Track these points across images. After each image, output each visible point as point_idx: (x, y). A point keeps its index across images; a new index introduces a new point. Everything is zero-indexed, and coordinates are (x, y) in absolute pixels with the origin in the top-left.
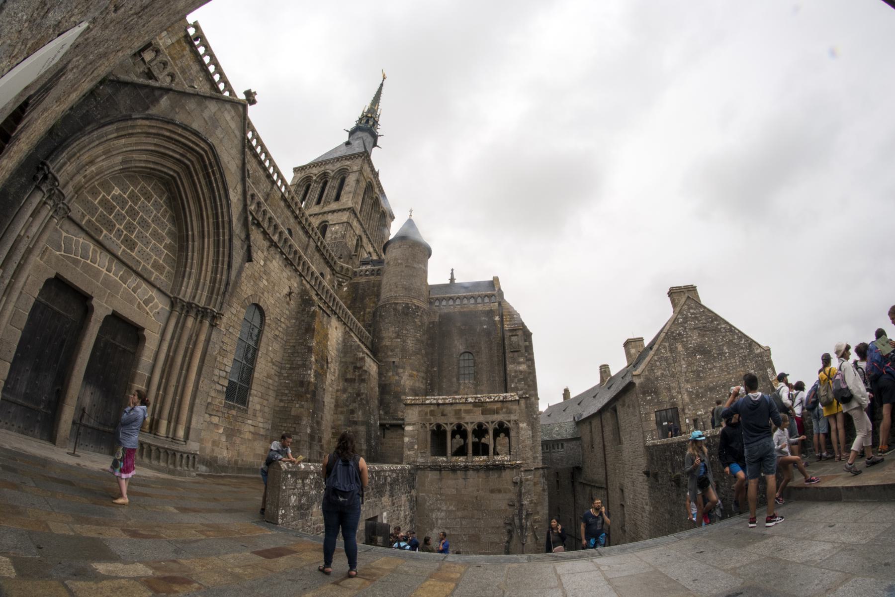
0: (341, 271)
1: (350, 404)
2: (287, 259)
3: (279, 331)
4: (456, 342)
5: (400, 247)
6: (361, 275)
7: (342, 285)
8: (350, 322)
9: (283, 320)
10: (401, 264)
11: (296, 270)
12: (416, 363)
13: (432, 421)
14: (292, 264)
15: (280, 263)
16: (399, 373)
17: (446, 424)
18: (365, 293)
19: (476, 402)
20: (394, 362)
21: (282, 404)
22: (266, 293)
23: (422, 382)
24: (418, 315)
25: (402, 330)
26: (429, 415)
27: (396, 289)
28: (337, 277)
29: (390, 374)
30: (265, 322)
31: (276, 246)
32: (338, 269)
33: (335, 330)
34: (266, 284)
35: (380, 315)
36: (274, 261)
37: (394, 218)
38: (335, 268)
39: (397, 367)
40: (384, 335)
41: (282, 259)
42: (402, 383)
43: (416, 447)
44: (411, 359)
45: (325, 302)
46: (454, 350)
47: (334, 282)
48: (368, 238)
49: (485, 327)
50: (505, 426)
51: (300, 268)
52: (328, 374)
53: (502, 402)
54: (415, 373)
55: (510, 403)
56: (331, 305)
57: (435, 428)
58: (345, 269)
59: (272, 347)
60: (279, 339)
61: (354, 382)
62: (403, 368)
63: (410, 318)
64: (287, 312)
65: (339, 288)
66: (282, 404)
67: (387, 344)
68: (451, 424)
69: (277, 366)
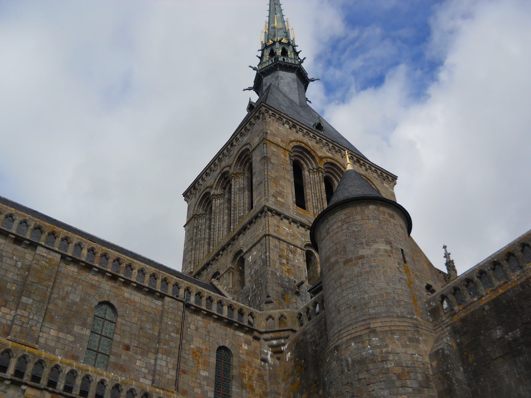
7: (281, 352)
10: (337, 262)
24: (388, 353)
28: (266, 340)
32: (261, 325)
38: (255, 327)
47: (262, 352)
58: (276, 318)
63: (371, 366)
65: (278, 359)
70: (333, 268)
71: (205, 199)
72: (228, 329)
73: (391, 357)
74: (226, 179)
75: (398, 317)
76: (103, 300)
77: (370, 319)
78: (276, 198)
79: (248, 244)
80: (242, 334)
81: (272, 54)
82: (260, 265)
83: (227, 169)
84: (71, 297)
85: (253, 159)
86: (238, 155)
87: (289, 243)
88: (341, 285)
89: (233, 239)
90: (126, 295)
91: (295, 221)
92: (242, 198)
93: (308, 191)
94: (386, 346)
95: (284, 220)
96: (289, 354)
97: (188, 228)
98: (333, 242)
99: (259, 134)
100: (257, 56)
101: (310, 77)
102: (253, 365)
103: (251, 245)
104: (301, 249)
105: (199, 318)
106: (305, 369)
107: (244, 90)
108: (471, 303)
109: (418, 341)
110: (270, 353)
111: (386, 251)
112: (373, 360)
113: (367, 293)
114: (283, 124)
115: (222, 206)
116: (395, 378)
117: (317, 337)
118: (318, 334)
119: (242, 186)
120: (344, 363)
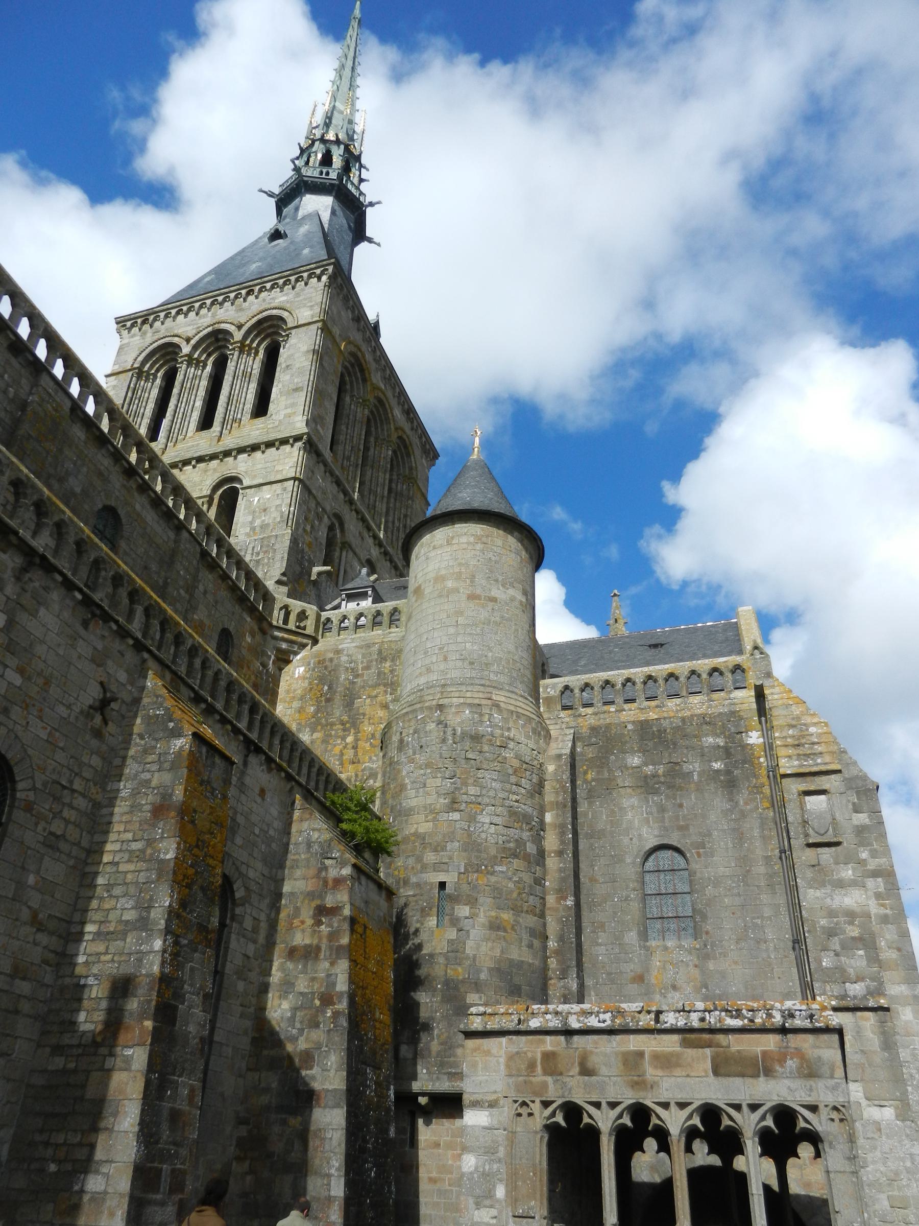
0: (286, 621)
1: (301, 1031)
2: (88, 602)
3: (67, 822)
4: (630, 815)
5: (449, 543)
6: (346, 628)
8: (305, 770)
9: (78, 785)
11: (123, 633)
12: (511, 885)
13: (552, 1093)
14: (106, 618)
15: (66, 614)
16: (458, 919)
17: (597, 1105)
18: (358, 680)
19: (692, 1030)
20: (442, 885)
21: (59, 1062)
22: (16, 712)
23: (530, 946)
25: (465, 784)
26: (539, 1069)
27: (442, 666)
29: (432, 922)
30: (14, 798)
31: (49, 568)
33: (259, 800)
34: (18, 680)
35: (401, 741)
36: (42, 611)
37: (436, 456)
39: (455, 899)
40: (413, 803)
41: (71, 604)
42: (468, 951)
43: (500, 1192)
44: (493, 873)
45: (224, 720)
46: (626, 841)
47: (264, 653)
48: (363, 520)
49: (717, 765)
50: (802, 1124)
51: (136, 627)
52: (233, 936)
53: (783, 1031)
54: (506, 916)
55: (810, 1038)
56: (242, 725)
57: (560, 1119)
59: (38, 872)
60: (63, 846)
61: (317, 957)
62: (472, 902)
63: (486, 748)
64: (96, 761)
66: (59, 1062)
67: (421, 830)
68: (613, 1105)
69: (52, 933)
70: (448, 596)
71: (163, 351)
72: (237, 607)
73: (511, 745)
74: (217, 340)
75: (522, 696)
76: (108, 503)
77: (491, 686)
78: (316, 425)
79: (255, 476)
80: (249, 619)
81: (327, 160)
82: (275, 518)
83: (231, 328)
84: (72, 481)
85: (292, 341)
86: (260, 316)
87: (318, 504)
88: (457, 625)
89: (227, 453)
90: (138, 507)
91: (332, 474)
92: (245, 389)
93: (343, 427)
94: (509, 729)
95: (321, 465)
96: (302, 669)
97: (115, 383)
98: (456, 559)
99: (312, 306)
100: (299, 144)
101: (369, 233)
102: (252, 668)
103: (261, 481)
104: (329, 517)
105: (210, 576)
106: (328, 700)
107: (261, 191)
108: (605, 712)
109: (539, 734)
110: (273, 657)
111: (521, 602)
112: (491, 740)
113: (491, 651)
114: (348, 308)
115: (197, 382)
116: (510, 771)
117: (360, 666)
118: (362, 662)
119: (249, 370)
120: (449, 731)
